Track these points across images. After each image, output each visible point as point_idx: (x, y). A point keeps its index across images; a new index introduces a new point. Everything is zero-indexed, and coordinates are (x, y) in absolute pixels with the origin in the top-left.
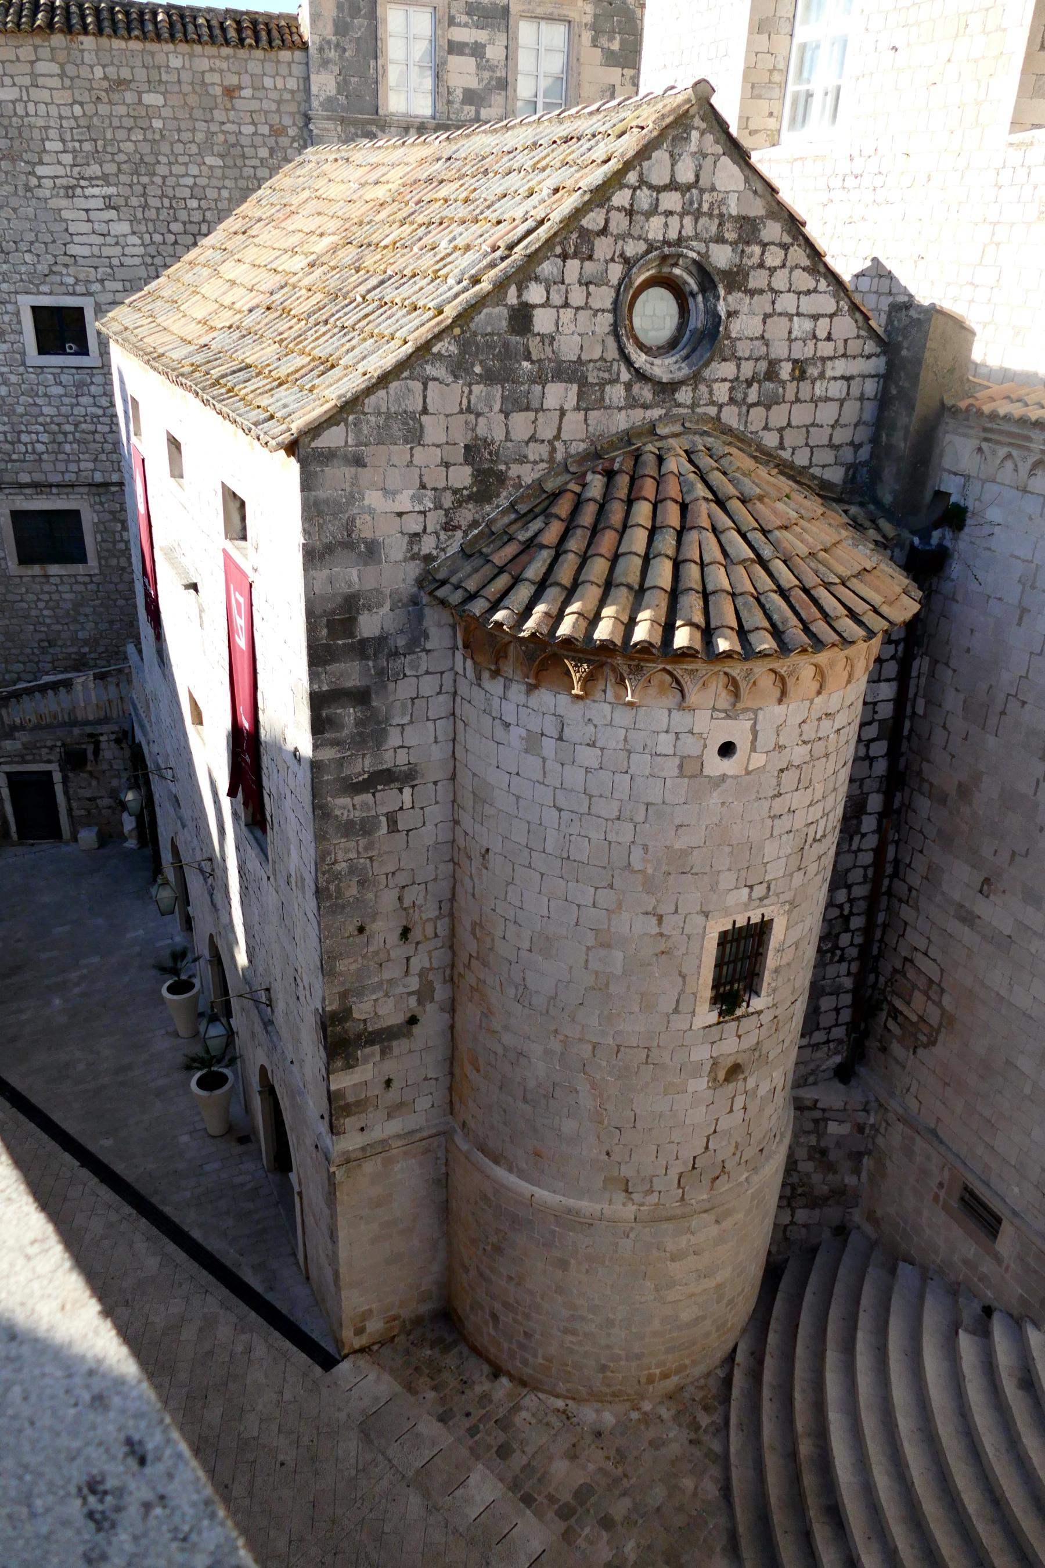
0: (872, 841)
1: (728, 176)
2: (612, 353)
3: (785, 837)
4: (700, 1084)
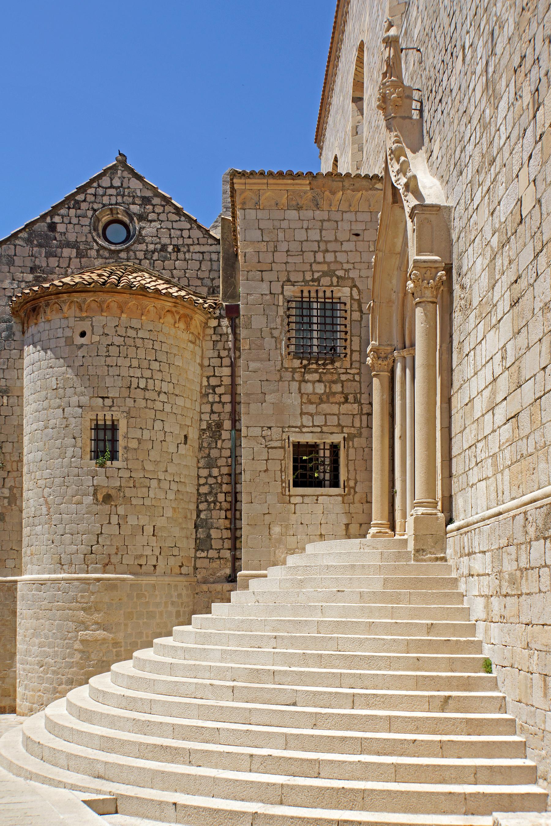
0: (228, 444)
1: (135, 184)
2: (90, 239)
3: (116, 377)
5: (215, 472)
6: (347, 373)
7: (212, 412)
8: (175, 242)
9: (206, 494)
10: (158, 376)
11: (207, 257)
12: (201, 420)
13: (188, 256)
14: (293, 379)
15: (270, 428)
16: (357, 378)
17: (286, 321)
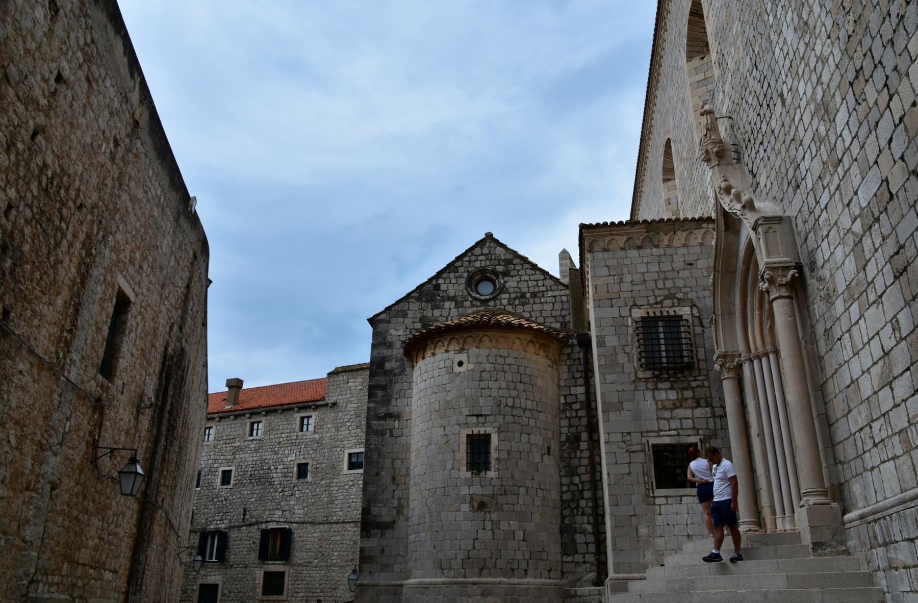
0: (586, 454)
1: (499, 250)
2: (465, 293)
4: (466, 507)
5: (576, 480)
6: (696, 380)
7: (570, 426)
8: (532, 290)
9: (569, 501)
10: (523, 395)
11: (558, 299)
12: (561, 433)
13: (542, 300)
14: (647, 389)
15: (629, 433)
16: (706, 384)
17: (636, 338)
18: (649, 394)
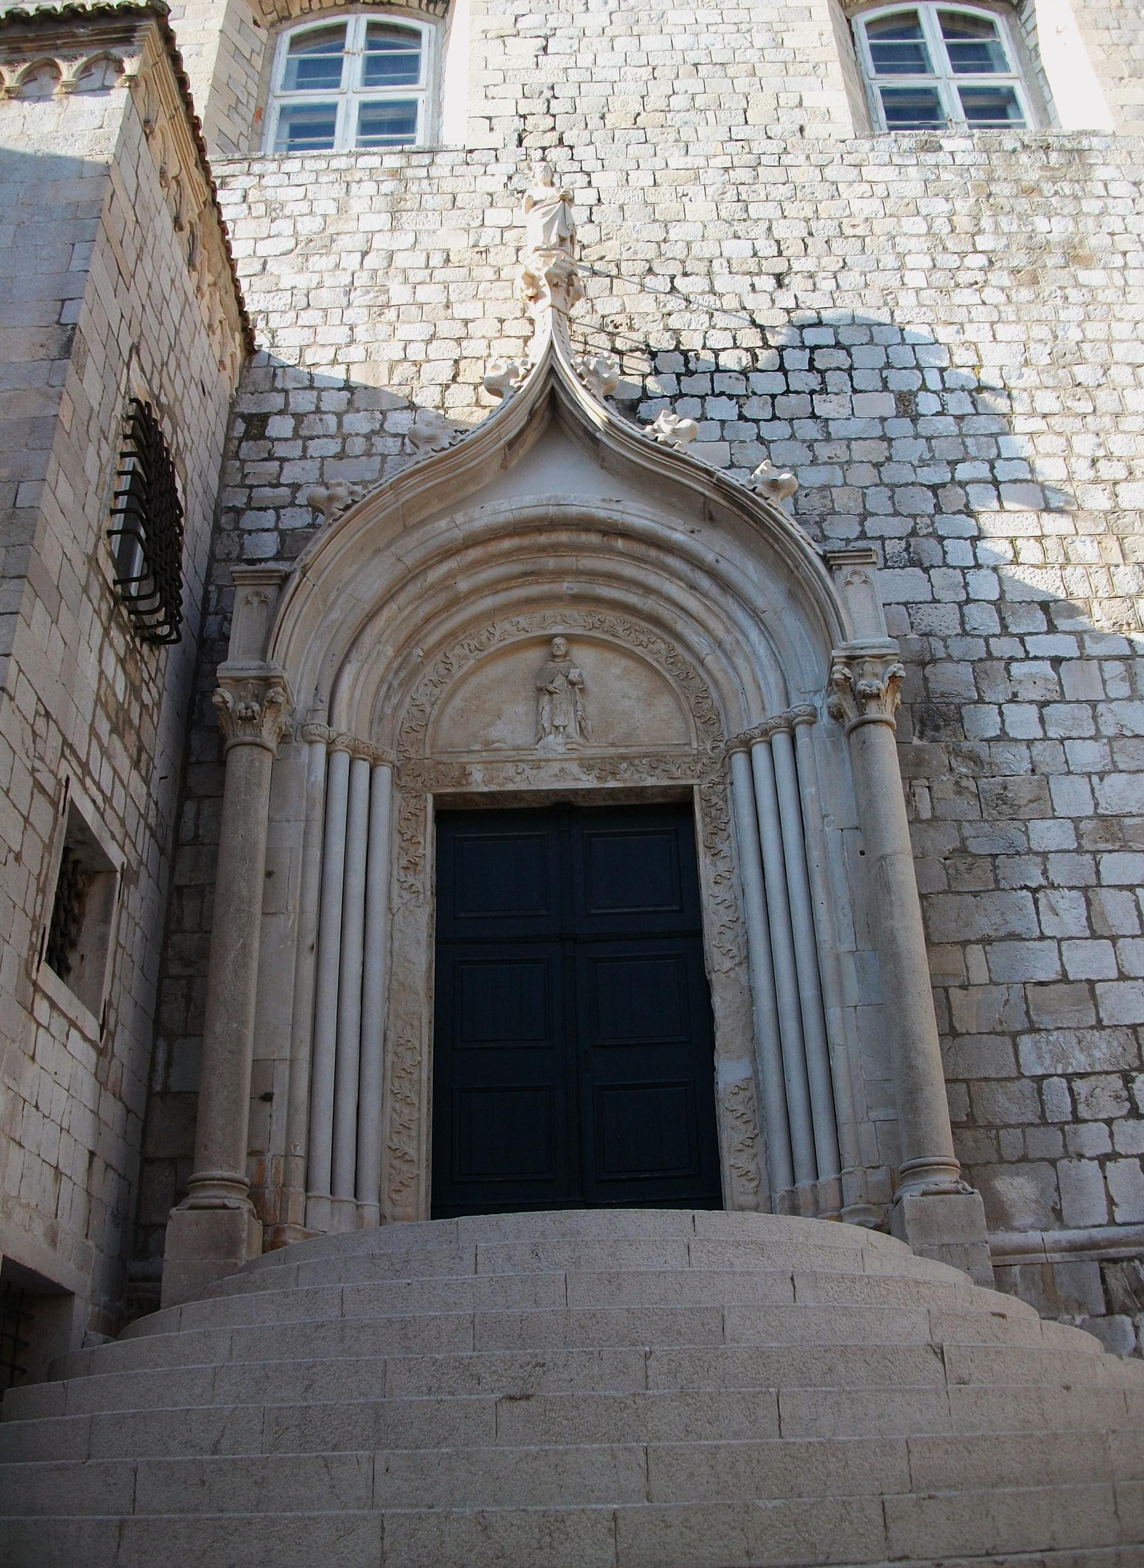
15: (47, 715)
18: (98, 631)
